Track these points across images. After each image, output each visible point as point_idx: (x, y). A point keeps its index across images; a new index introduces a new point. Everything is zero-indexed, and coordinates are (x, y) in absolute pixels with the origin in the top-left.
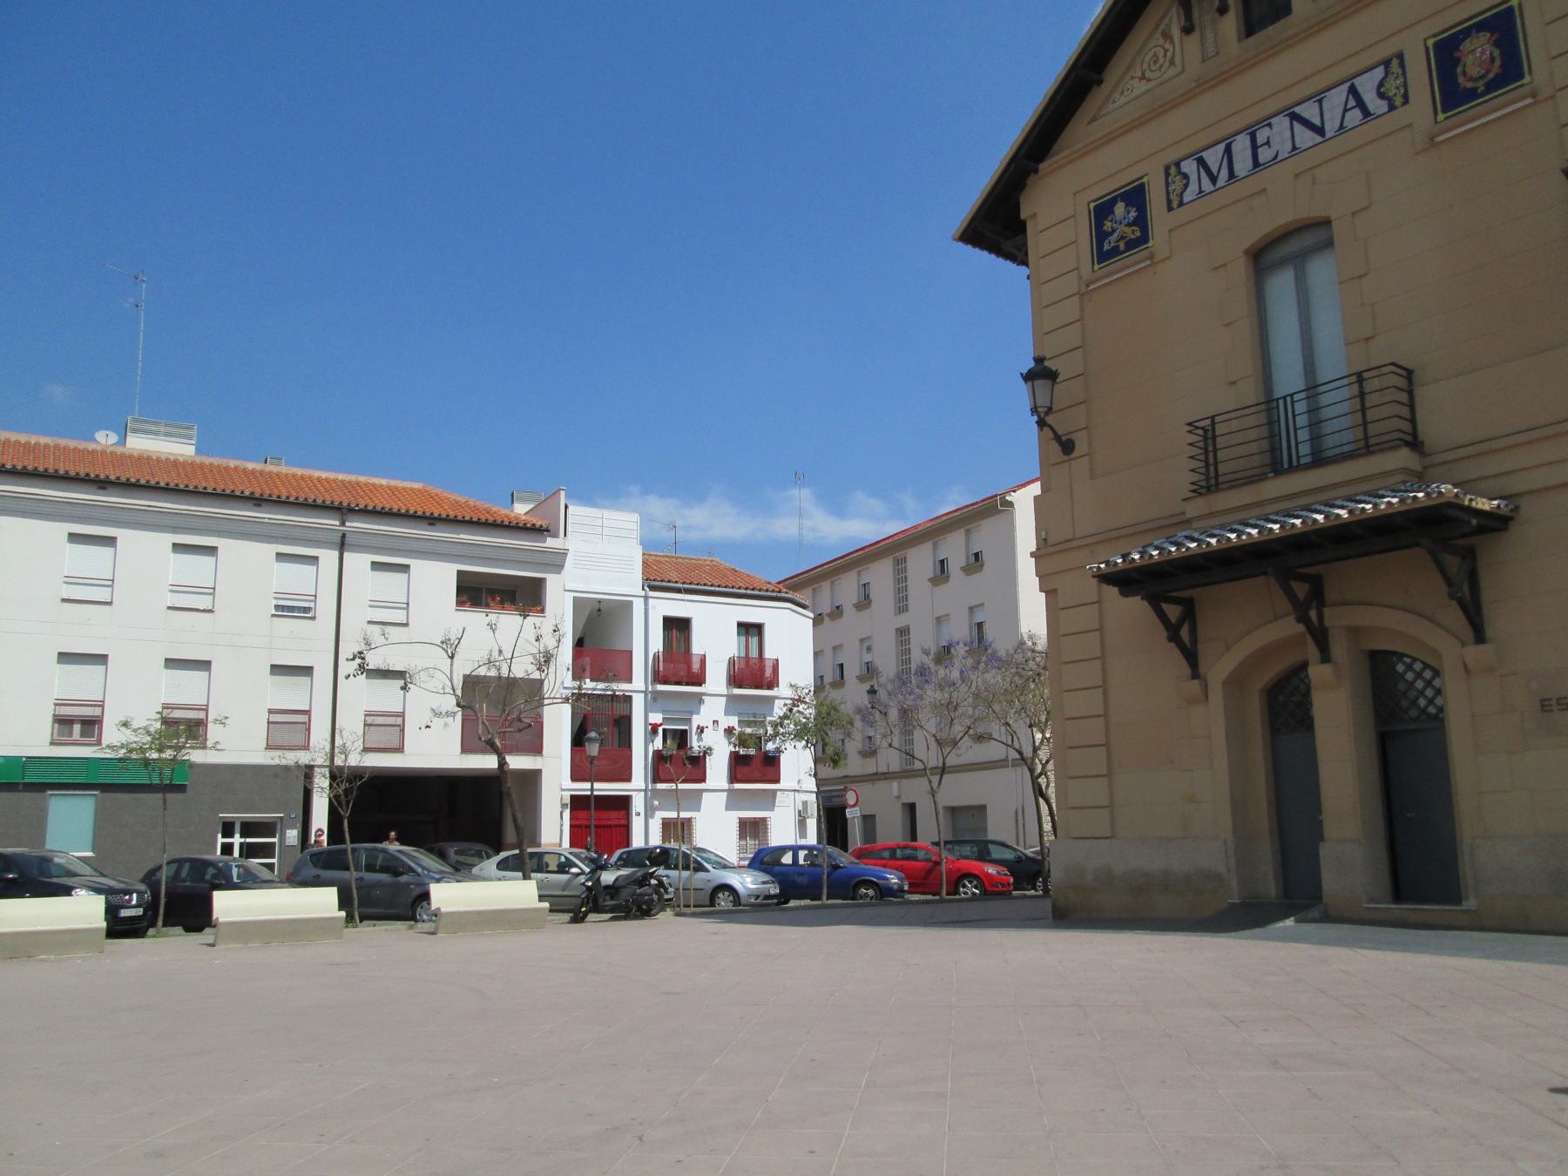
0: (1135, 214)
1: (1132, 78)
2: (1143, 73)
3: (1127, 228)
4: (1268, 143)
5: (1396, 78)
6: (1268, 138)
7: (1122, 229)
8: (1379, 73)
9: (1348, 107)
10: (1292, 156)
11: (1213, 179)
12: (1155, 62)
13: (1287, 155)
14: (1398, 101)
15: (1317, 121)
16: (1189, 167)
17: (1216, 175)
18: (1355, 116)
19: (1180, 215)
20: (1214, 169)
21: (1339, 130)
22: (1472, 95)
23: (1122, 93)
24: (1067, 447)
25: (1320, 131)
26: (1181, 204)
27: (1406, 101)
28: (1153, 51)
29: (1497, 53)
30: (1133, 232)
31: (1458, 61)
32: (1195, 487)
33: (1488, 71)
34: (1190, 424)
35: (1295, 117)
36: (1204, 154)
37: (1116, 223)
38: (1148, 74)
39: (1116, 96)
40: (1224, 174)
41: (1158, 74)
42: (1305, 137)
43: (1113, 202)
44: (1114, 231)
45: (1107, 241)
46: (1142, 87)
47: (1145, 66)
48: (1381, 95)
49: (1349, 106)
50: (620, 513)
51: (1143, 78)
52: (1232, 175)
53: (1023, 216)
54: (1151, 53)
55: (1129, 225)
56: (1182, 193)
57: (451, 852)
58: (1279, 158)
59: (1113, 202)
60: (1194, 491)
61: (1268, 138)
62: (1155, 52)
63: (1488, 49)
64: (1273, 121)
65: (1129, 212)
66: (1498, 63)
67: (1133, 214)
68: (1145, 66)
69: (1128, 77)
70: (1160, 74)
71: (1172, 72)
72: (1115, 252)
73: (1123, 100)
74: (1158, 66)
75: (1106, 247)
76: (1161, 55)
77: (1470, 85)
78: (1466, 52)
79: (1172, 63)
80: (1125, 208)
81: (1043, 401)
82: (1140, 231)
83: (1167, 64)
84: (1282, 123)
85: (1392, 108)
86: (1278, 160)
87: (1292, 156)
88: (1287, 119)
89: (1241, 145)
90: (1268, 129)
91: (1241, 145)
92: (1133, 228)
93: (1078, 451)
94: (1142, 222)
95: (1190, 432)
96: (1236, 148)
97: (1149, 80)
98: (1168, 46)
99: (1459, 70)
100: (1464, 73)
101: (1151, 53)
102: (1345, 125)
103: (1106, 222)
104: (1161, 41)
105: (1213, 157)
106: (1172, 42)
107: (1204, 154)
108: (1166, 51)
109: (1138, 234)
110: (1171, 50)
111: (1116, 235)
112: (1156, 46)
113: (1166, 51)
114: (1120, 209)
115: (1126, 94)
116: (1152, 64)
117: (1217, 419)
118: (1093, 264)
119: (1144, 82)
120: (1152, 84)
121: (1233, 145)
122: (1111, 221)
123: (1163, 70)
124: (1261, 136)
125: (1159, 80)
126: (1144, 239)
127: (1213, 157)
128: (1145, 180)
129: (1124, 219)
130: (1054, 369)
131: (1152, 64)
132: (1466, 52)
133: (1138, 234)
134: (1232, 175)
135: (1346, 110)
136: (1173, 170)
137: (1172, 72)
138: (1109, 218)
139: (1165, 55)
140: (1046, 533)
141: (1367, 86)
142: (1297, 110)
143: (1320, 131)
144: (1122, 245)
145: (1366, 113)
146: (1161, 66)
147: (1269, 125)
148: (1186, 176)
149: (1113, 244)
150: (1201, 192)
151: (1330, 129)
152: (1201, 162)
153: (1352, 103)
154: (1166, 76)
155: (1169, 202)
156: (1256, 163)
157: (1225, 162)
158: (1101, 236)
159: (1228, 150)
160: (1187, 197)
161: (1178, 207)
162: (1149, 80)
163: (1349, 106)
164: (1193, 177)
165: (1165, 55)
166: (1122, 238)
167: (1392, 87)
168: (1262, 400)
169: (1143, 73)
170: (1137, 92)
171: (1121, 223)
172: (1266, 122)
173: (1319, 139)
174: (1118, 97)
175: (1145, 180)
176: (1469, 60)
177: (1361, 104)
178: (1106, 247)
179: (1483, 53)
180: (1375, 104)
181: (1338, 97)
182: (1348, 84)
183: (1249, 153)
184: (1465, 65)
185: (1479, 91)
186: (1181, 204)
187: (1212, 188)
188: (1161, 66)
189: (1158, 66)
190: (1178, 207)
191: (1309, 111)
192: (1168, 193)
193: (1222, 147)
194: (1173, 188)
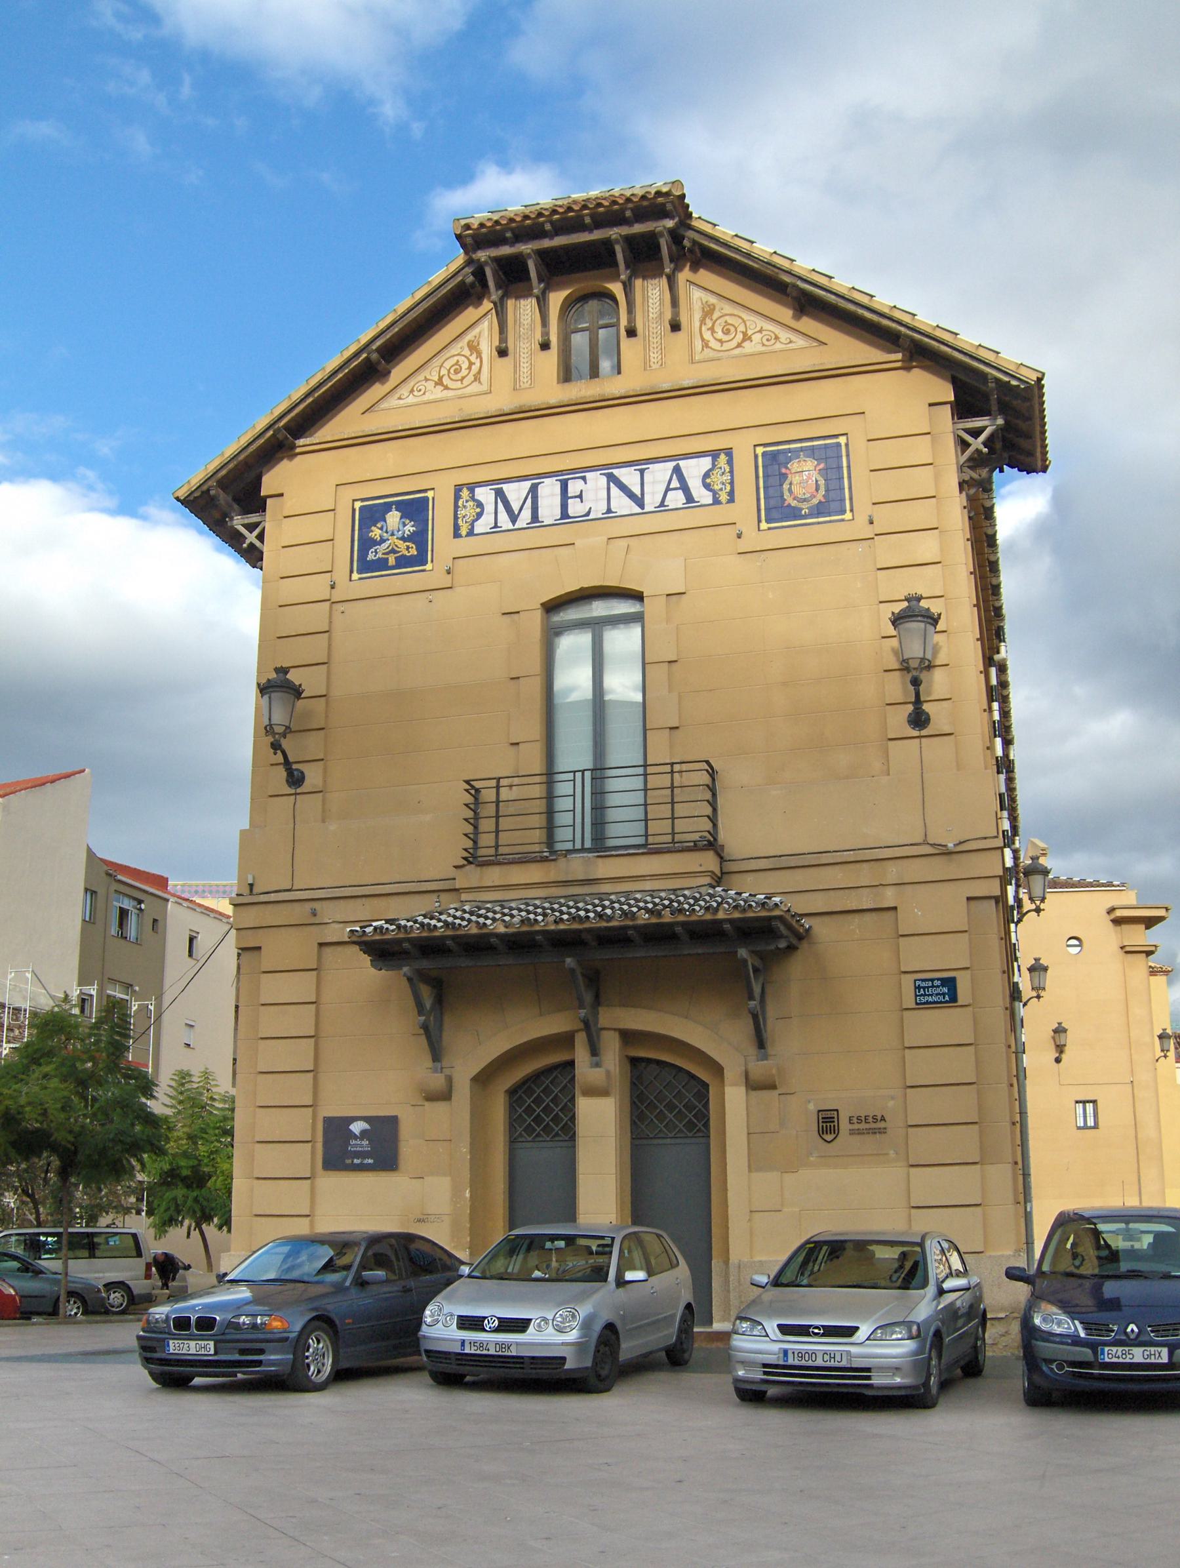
0: (412, 529)
1: (426, 380)
2: (441, 378)
3: (401, 542)
4: (580, 496)
5: (723, 473)
6: (581, 491)
7: (393, 541)
8: (706, 462)
9: (671, 487)
10: (528, 528)
11: (514, 518)
12: (456, 372)
13: (601, 516)
14: (724, 497)
15: (637, 490)
16: (485, 495)
17: (516, 513)
18: (676, 499)
19: (465, 545)
20: (515, 507)
21: (658, 507)
22: (795, 514)
23: (412, 391)
24: (295, 779)
25: (640, 502)
26: (471, 533)
27: (731, 500)
28: (456, 358)
29: (822, 482)
30: (408, 548)
31: (784, 477)
32: (468, 855)
33: (813, 496)
34: (467, 782)
35: (611, 478)
36: (505, 487)
37: (387, 532)
38: (446, 381)
39: (404, 391)
40: (526, 515)
41: (459, 385)
42: (622, 504)
43: (387, 507)
44: (383, 541)
45: (373, 550)
46: (438, 393)
47: (444, 372)
48: (707, 486)
49: (672, 486)
50: (576, 619)
51: (439, 382)
52: (535, 517)
53: (264, 492)
54: (453, 360)
55: (403, 539)
56: (474, 521)
57: (1036, 1310)
58: (591, 516)
59: (387, 507)
60: (465, 859)
61: (581, 491)
62: (458, 361)
63: (815, 475)
64: (588, 475)
65: (405, 525)
66: (822, 492)
67: (410, 528)
68: (444, 372)
69: (421, 377)
70: (461, 386)
71: (475, 388)
72: (381, 565)
73: (411, 400)
74: (459, 376)
75: (371, 556)
76: (465, 365)
77: (794, 503)
78: (793, 471)
79: (477, 378)
80: (401, 519)
81: (279, 717)
82: (417, 549)
83: (471, 378)
84: (597, 481)
85: (716, 501)
86: (590, 517)
87: (528, 528)
88: (604, 479)
89: (549, 491)
90: (582, 482)
91: (549, 491)
92: (408, 544)
93: (307, 786)
94: (420, 538)
95: (467, 790)
96: (542, 491)
97: (446, 388)
98: (473, 358)
99: (786, 486)
100: (790, 490)
101: (453, 360)
102: (666, 504)
103: (373, 528)
104: (467, 352)
105: (516, 493)
106: (479, 356)
107: (505, 487)
108: (471, 364)
109: (414, 552)
110: (478, 364)
111: (385, 546)
112: (458, 355)
113: (471, 364)
114: (393, 518)
115: (416, 393)
116: (452, 371)
117: (503, 782)
118: (351, 572)
119: (440, 388)
120: (450, 394)
121: (539, 486)
122: (381, 529)
123: (466, 382)
124: (574, 487)
125: (460, 392)
126: (420, 559)
127: (516, 493)
128: (430, 494)
129: (399, 531)
130: (297, 684)
131: (452, 371)
132: (793, 471)
133: (414, 552)
134: (535, 517)
135: (668, 489)
136: (465, 493)
137: (475, 388)
138: (379, 525)
139: (470, 368)
140: (254, 878)
141: (694, 470)
142: (616, 472)
143: (640, 502)
144: (392, 560)
145: (689, 498)
146: (463, 378)
147: (584, 478)
148: (480, 505)
149: (380, 555)
150: (496, 526)
151: (651, 502)
152: (500, 494)
153: (675, 483)
154: (469, 390)
155: (456, 528)
156: (565, 514)
157: (500, 505)
158: (367, 543)
159: (534, 490)
160: (480, 527)
161: (466, 536)
162: (446, 388)
163: (672, 486)
164: (489, 508)
165: (470, 368)
166: (393, 551)
167: (718, 480)
168: (545, 772)
169: (441, 378)
170: (429, 397)
171: (393, 535)
172: (581, 472)
173: (638, 510)
174: (406, 394)
175: (430, 494)
176: (796, 479)
177: (685, 488)
178: (371, 556)
179: (809, 478)
180: (703, 496)
181: (660, 474)
182: (674, 463)
183: (557, 500)
184: (791, 484)
185: (803, 512)
186: (471, 533)
187: (510, 526)
188: (463, 378)
189: (459, 376)
190: (466, 536)
191: (628, 477)
192: (456, 518)
193: (527, 485)
194: (725, 478)
